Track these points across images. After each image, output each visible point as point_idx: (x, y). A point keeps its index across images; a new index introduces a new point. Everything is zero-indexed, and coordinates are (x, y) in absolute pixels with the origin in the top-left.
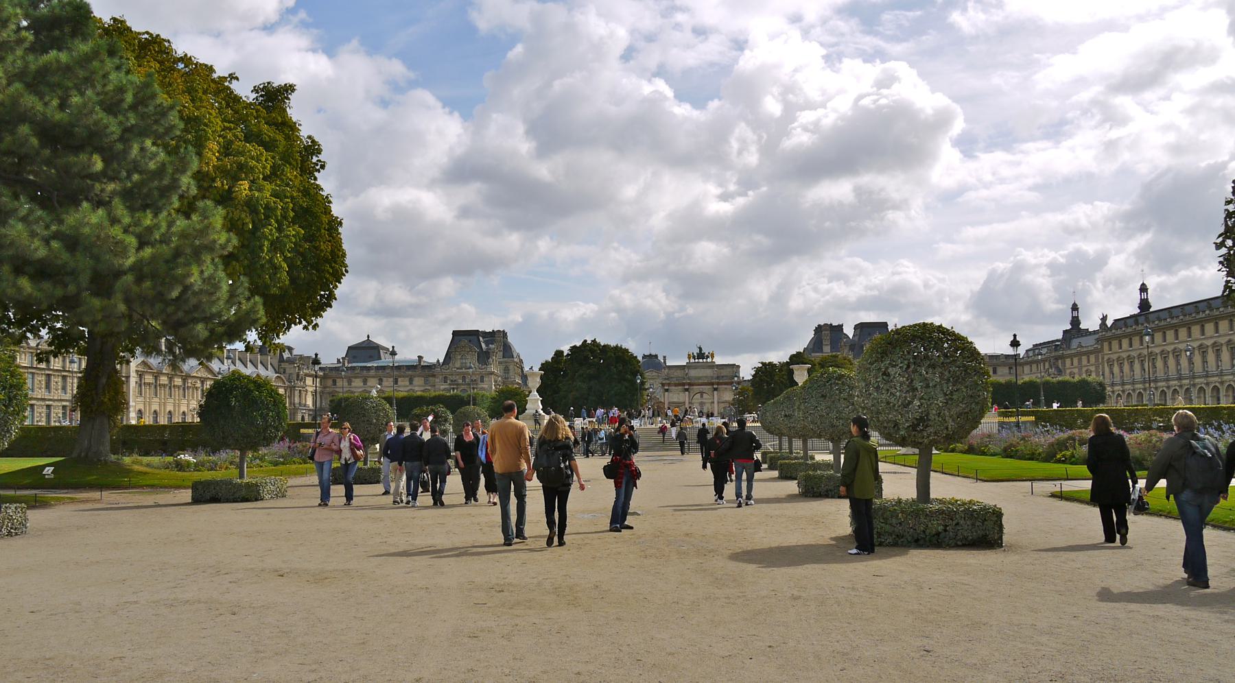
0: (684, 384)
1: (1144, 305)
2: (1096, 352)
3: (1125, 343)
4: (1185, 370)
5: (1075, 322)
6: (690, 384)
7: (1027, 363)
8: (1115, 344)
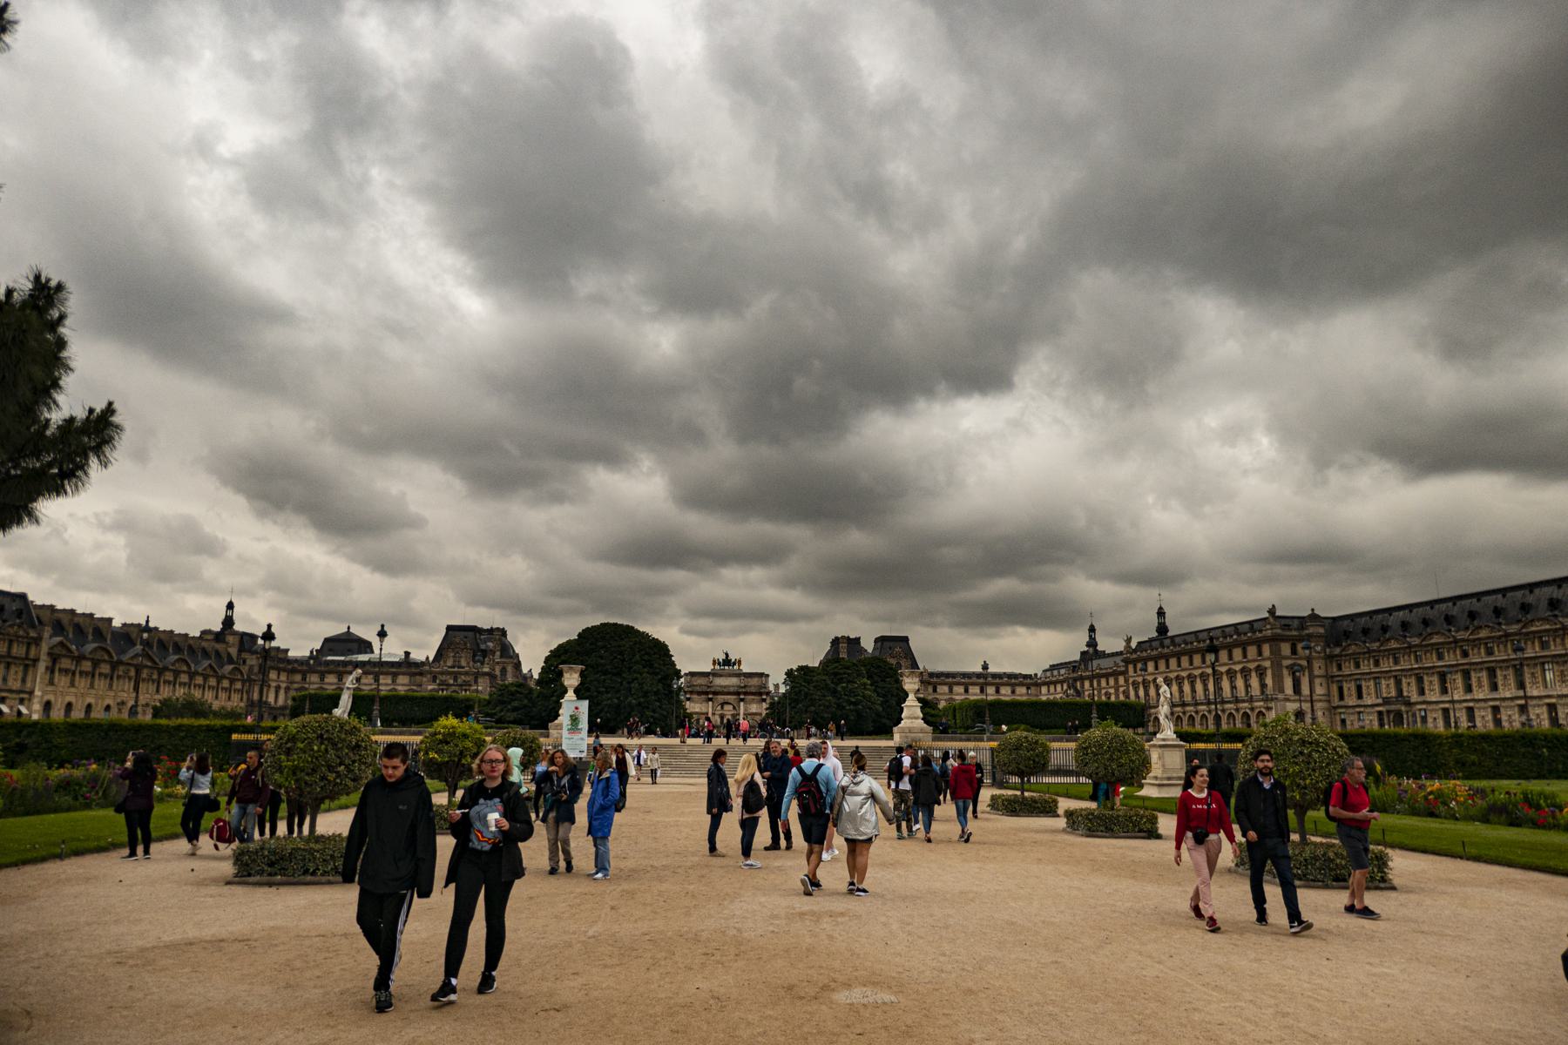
0: (707, 693)
1: (1162, 629)
3: (1173, 662)
4: (1241, 692)
6: (715, 693)
7: (1045, 684)
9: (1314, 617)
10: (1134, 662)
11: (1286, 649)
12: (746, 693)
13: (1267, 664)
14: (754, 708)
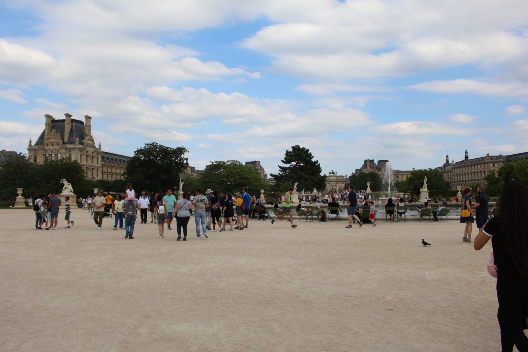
1: (466, 157)
2: (450, 172)
5: (447, 161)
8: (456, 170)
9: (500, 156)
10: (454, 168)
11: (491, 165)
13: (486, 170)
14: (341, 185)
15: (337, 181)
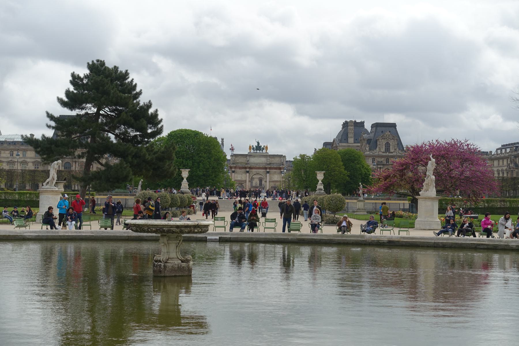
0: (246, 168)
6: (250, 168)
12: (270, 168)
15: (268, 168)
